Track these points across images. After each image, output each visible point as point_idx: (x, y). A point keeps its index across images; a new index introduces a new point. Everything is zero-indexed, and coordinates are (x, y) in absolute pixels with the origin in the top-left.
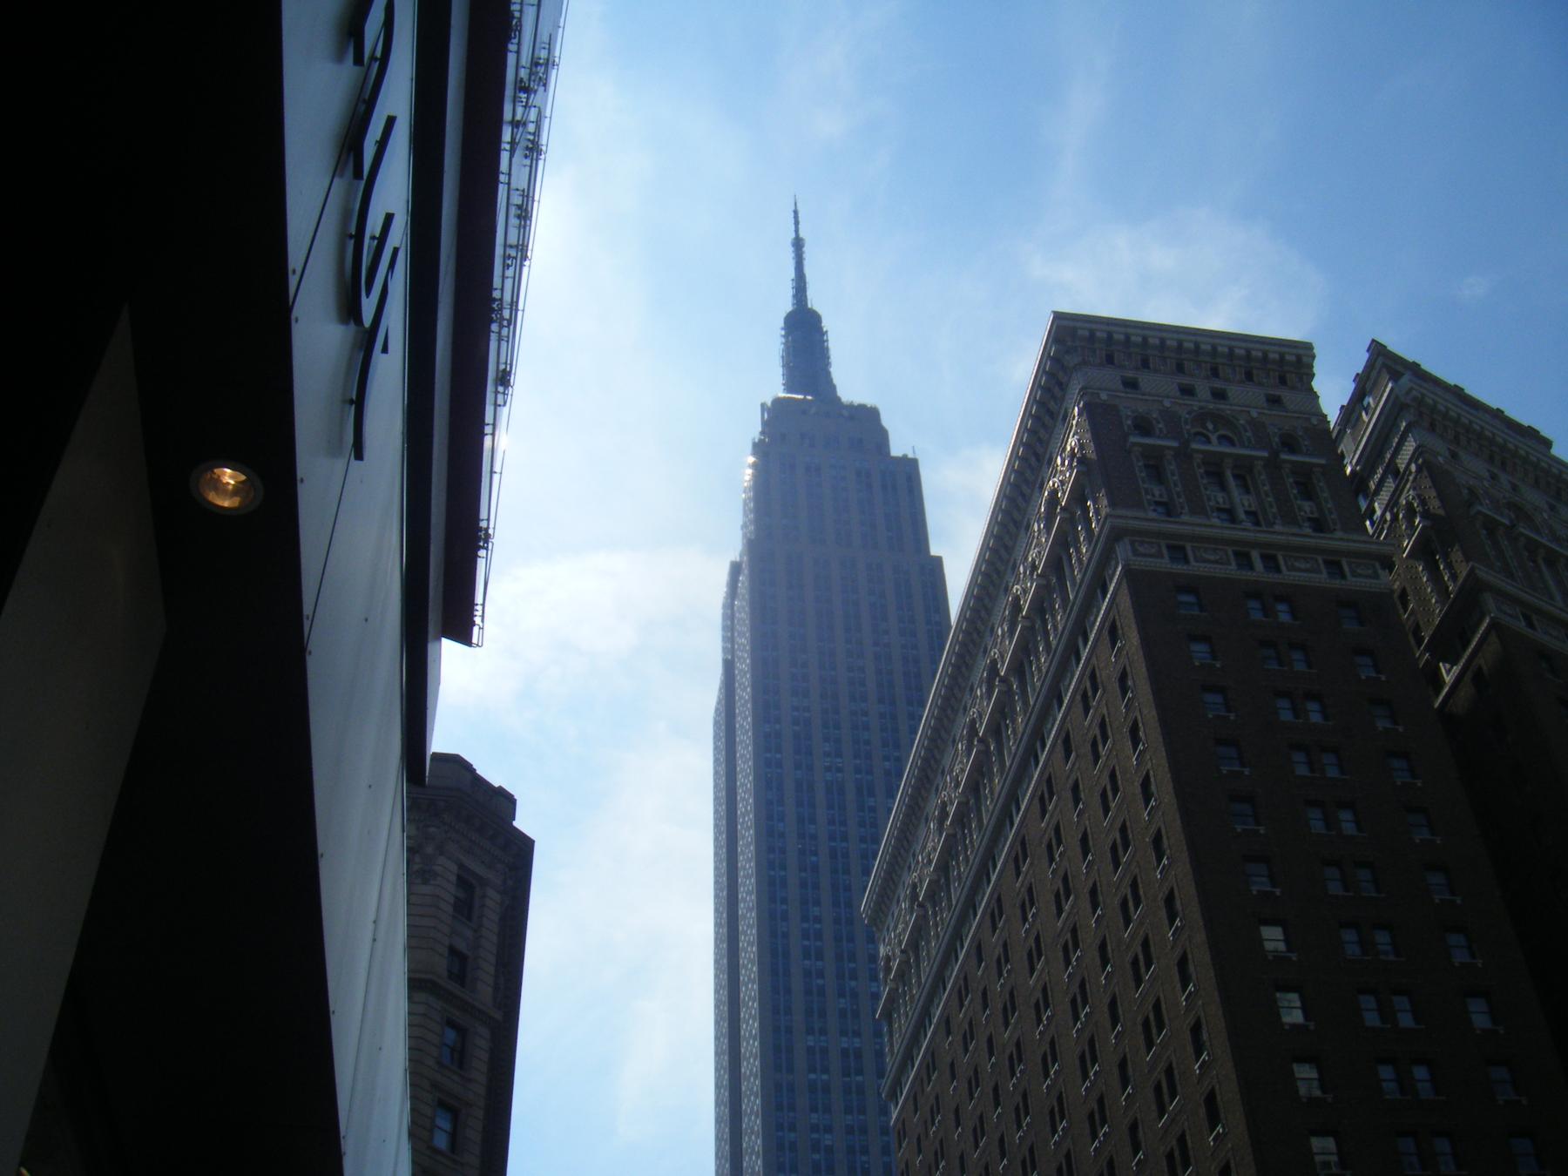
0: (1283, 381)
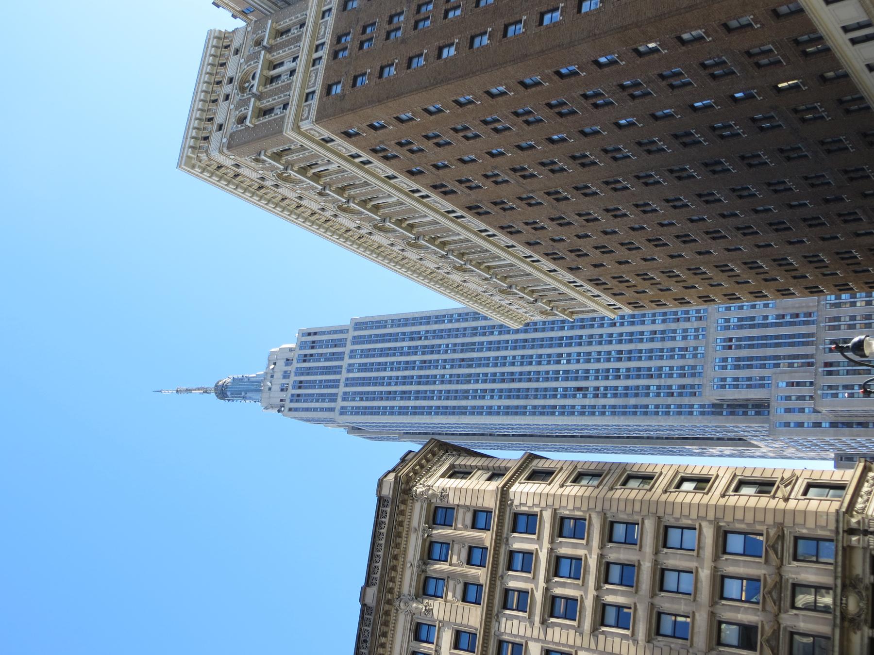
0: (227, 47)
